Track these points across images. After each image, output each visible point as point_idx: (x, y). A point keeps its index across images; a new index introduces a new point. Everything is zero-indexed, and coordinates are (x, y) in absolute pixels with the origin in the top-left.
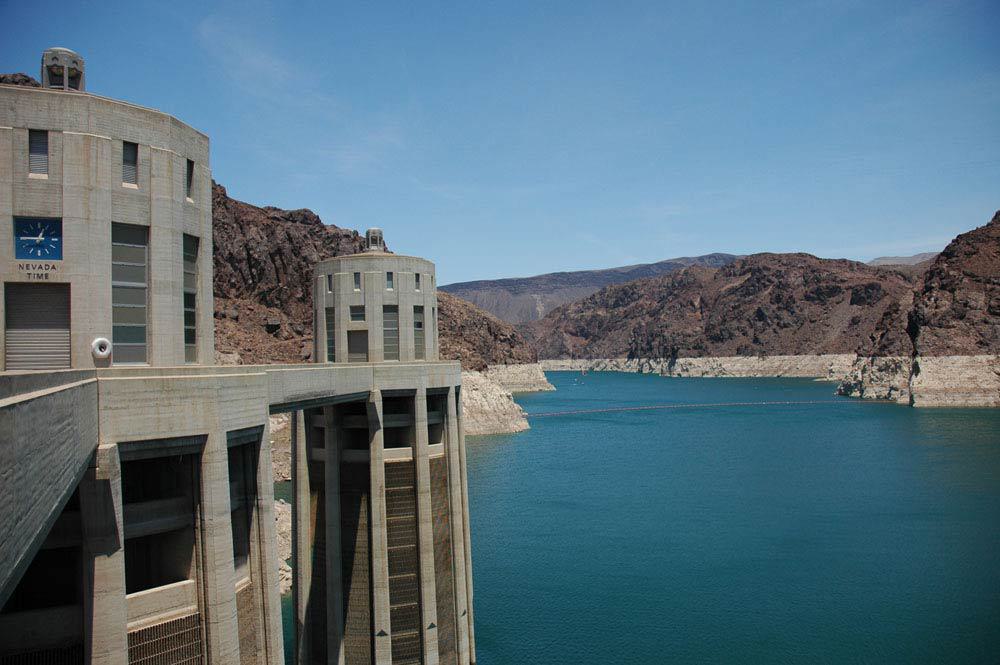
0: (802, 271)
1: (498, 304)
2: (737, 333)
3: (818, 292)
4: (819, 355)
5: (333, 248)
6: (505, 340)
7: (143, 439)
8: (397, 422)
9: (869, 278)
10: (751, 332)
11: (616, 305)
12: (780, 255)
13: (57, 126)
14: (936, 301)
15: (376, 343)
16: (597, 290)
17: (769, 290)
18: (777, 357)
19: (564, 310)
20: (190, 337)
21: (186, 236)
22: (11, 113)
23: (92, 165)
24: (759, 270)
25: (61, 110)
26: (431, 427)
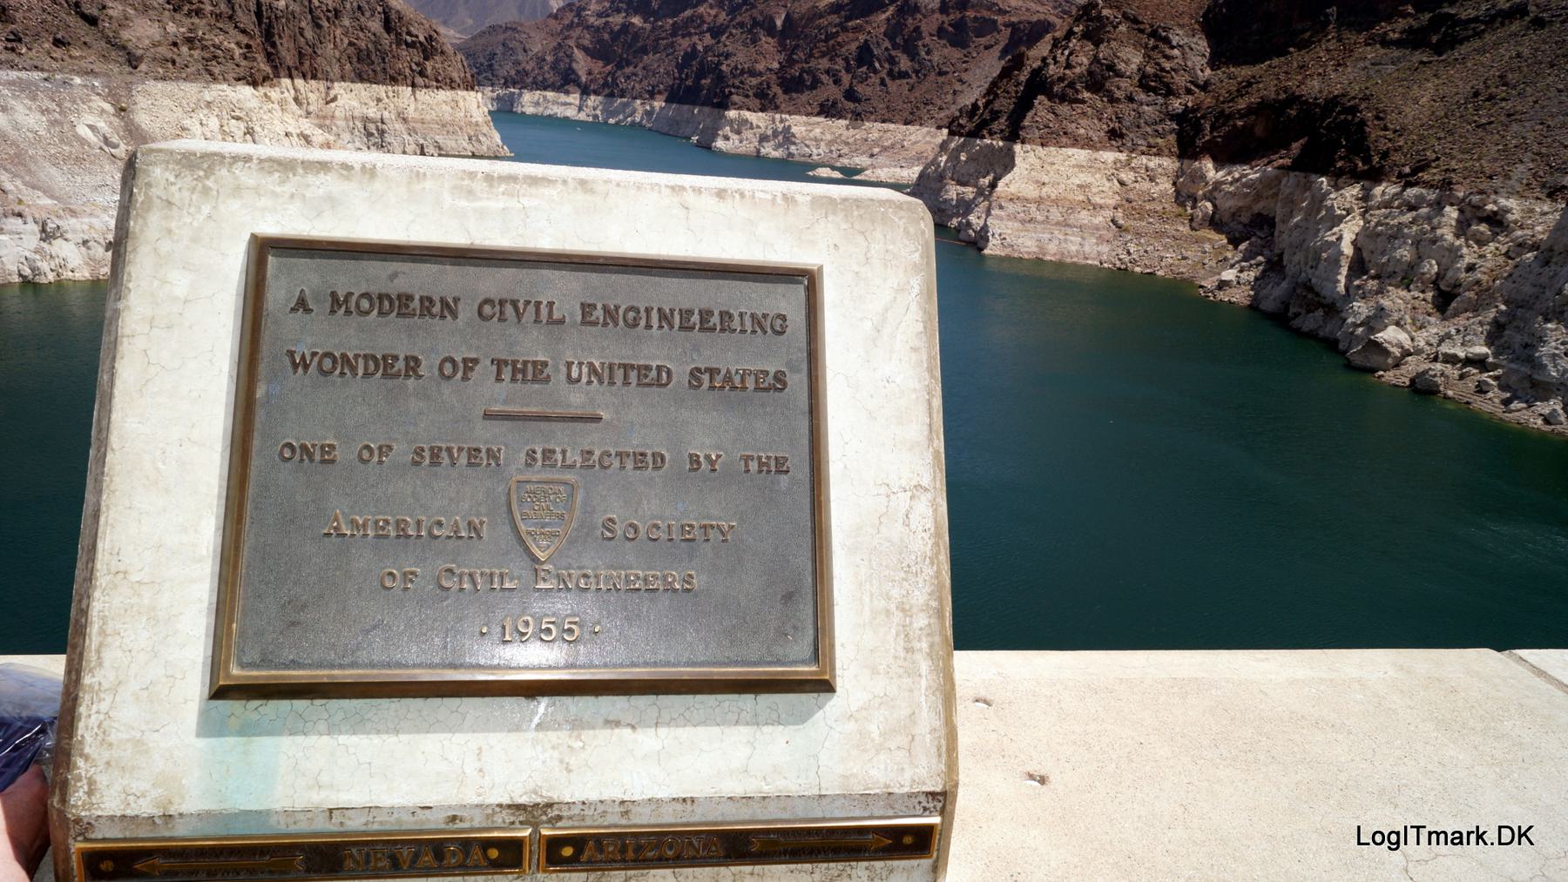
2: (824, 78)
3: (960, 25)
10: (846, 79)
18: (878, 125)
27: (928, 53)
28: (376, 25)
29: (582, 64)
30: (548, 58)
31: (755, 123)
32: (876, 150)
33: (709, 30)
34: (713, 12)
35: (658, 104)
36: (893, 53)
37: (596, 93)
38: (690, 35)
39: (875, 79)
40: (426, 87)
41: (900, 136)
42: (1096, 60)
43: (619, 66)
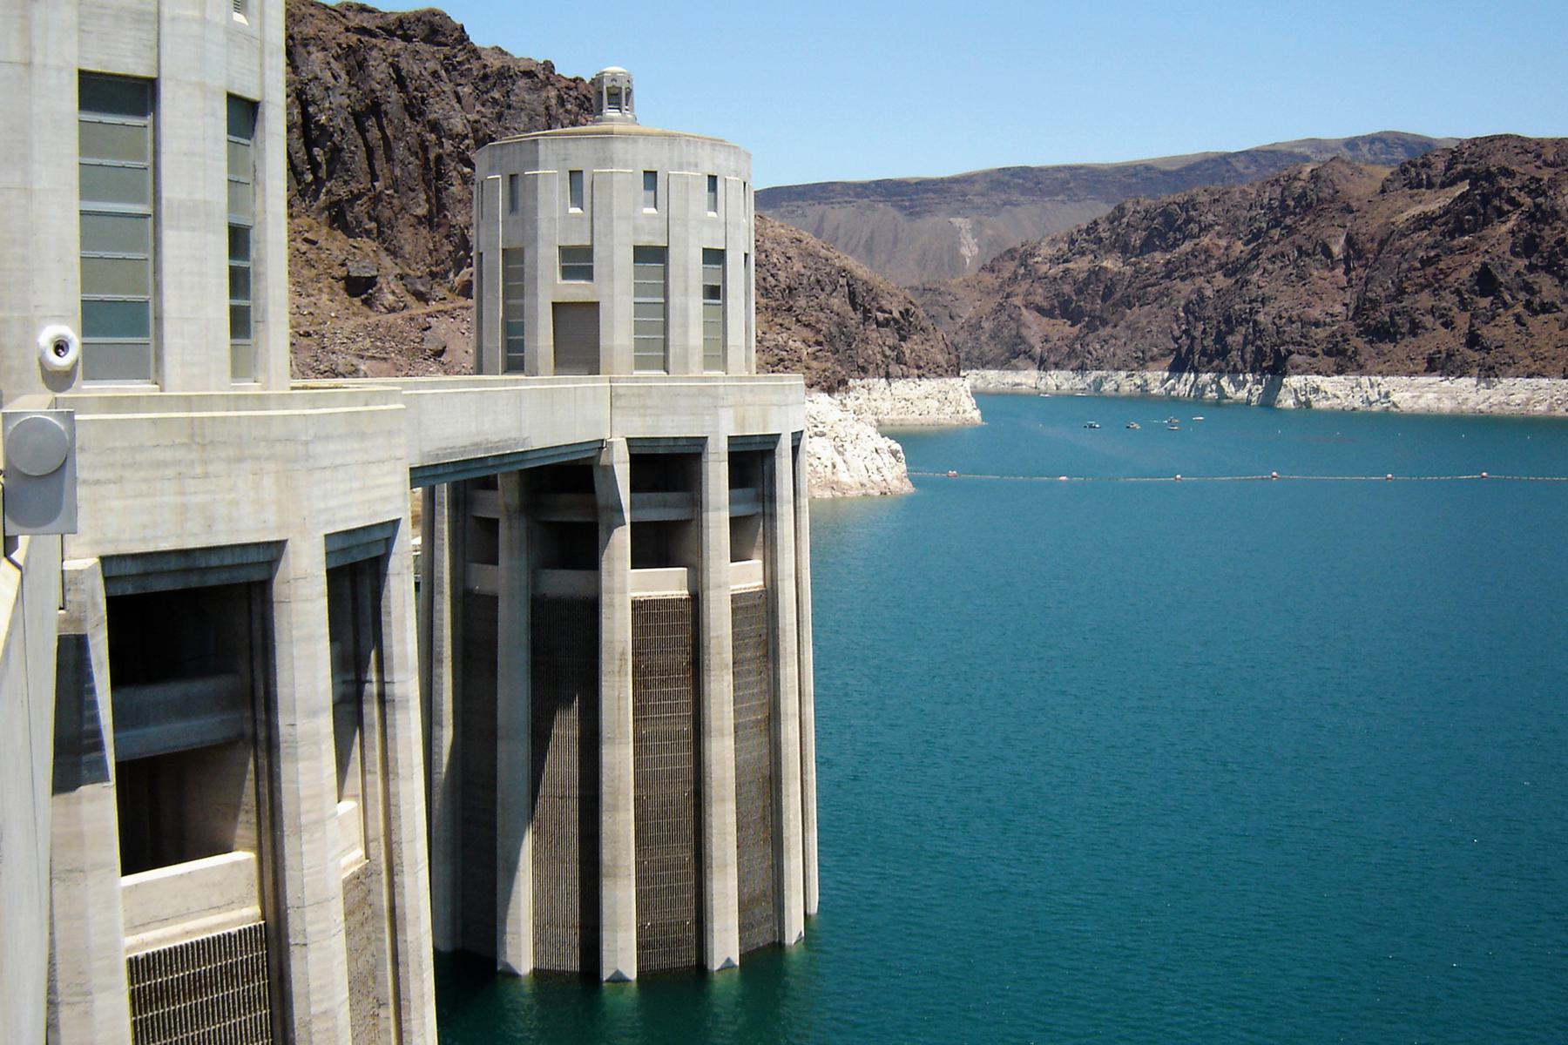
1: (872, 238)
2: (1428, 320)
5: (495, 102)
6: (886, 323)
7: (151, 548)
10: (1462, 321)
11: (1147, 247)
12: (1540, 143)
15: (618, 334)
16: (1104, 210)
17: (1509, 225)
18: (1522, 382)
19: (1023, 257)
20: (241, 323)
21: (233, 99)
24: (1489, 176)
26: (736, 523)
28: (838, 302)
30: (985, 325)
31: (1330, 390)
33: (1221, 267)
34: (1223, 243)
36: (1530, 278)
40: (905, 376)
43: (1091, 328)
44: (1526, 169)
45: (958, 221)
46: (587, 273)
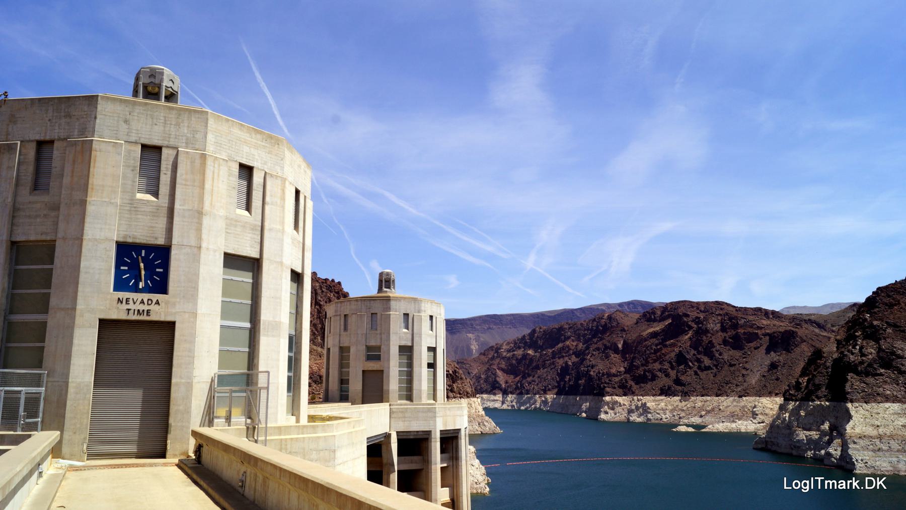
0: (719, 318)
2: (659, 374)
3: (736, 337)
4: (740, 397)
8: (412, 464)
9: (783, 326)
10: (673, 373)
12: (698, 303)
13: (172, 142)
14: (861, 348)
16: (527, 331)
18: (701, 398)
19: (497, 349)
22: (125, 126)
23: (208, 186)
25: (178, 125)
27: (720, 354)
29: (502, 378)
31: (622, 402)
32: (703, 413)
34: (575, 344)
35: (550, 397)
36: (699, 356)
37: (512, 393)
38: (563, 357)
39: (690, 372)
41: (715, 404)
42: (880, 350)
43: (524, 377)
44: (693, 314)
45: (470, 335)
46: (378, 358)
